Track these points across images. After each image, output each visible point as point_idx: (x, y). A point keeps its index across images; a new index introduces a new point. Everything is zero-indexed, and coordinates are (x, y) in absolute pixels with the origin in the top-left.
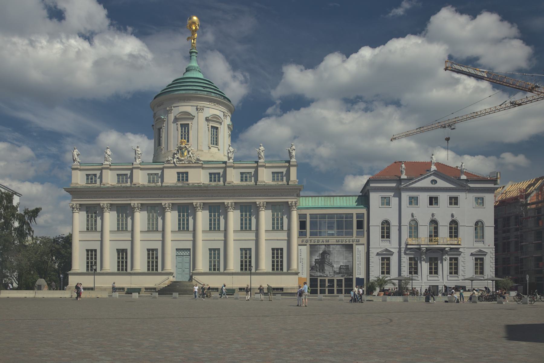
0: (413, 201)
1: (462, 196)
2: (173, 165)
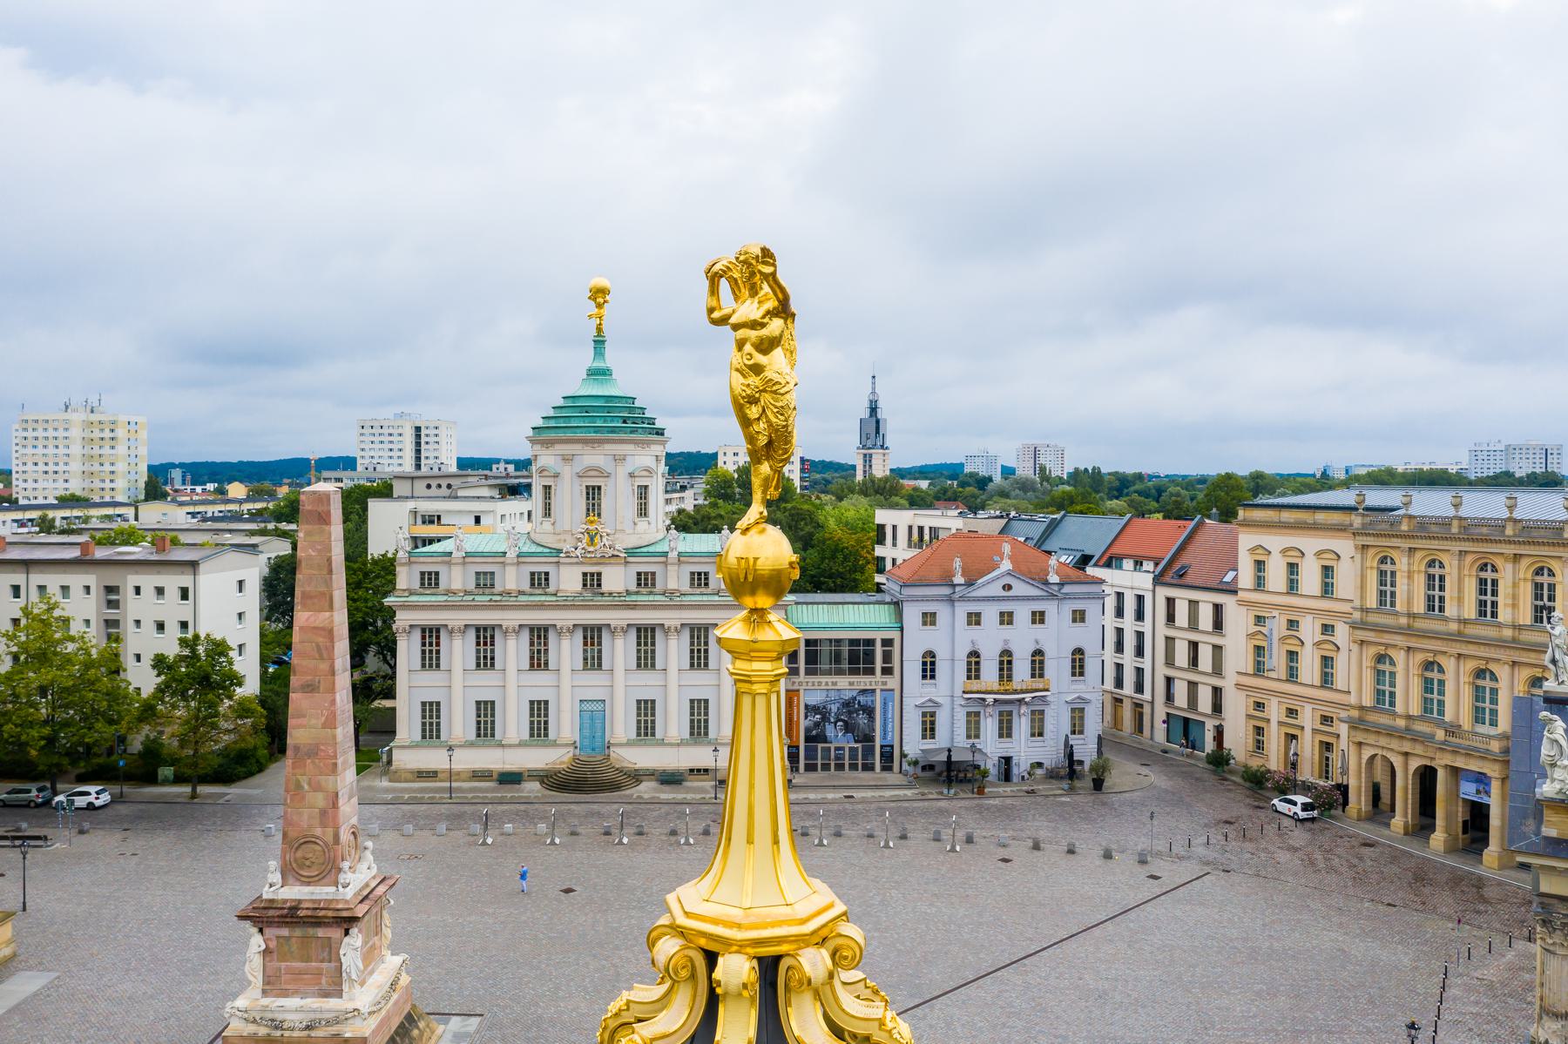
0: (974, 619)
1: (1050, 608)
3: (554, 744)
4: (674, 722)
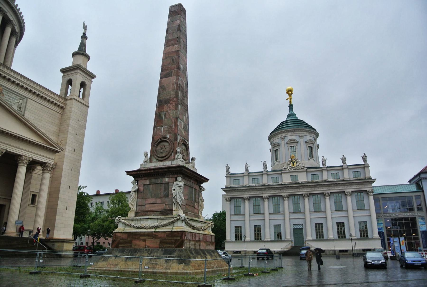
2: (288, 171)
3: (284, 241)
4: (331, 232)
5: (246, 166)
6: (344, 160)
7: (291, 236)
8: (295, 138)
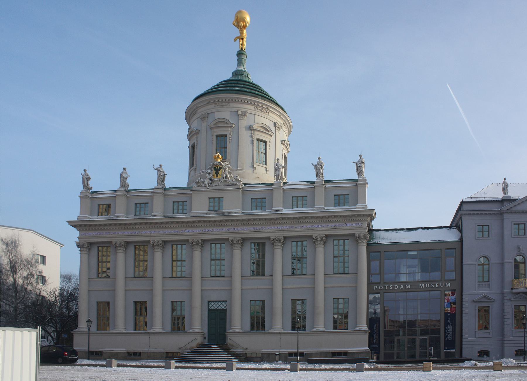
5: (121, 175)
6: (318, 168)
7: (202, 325)
8: (228, 118)
